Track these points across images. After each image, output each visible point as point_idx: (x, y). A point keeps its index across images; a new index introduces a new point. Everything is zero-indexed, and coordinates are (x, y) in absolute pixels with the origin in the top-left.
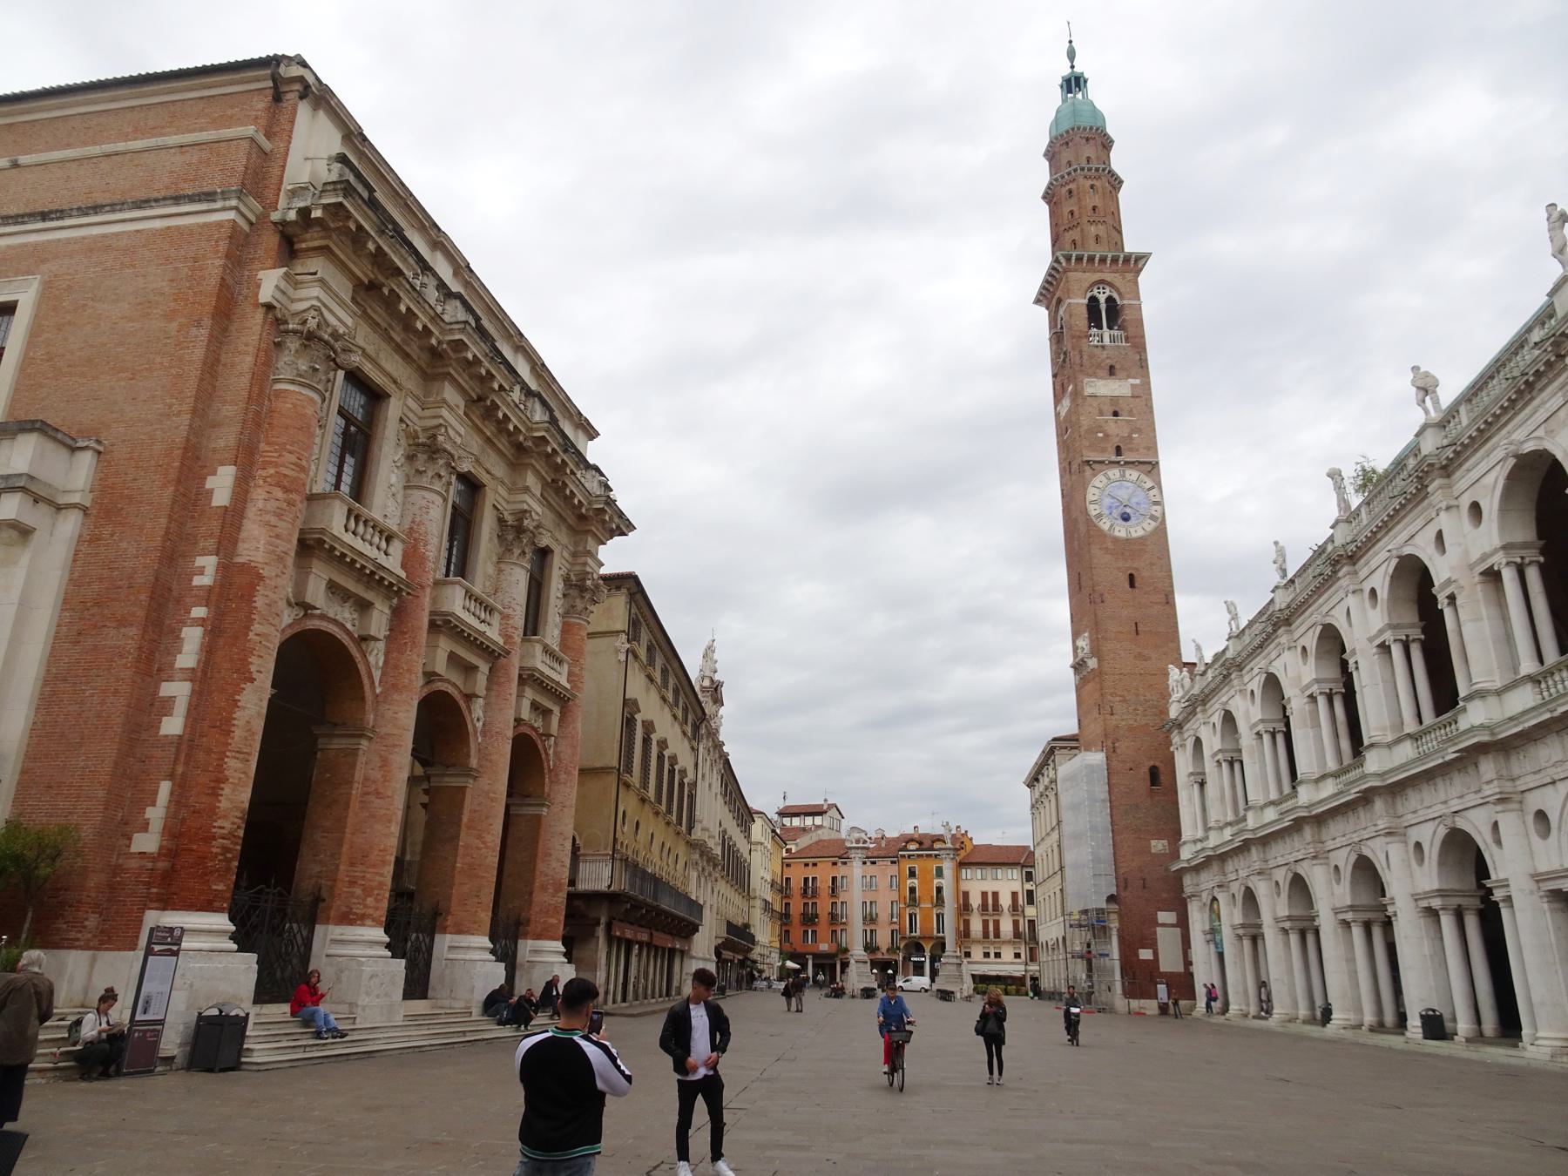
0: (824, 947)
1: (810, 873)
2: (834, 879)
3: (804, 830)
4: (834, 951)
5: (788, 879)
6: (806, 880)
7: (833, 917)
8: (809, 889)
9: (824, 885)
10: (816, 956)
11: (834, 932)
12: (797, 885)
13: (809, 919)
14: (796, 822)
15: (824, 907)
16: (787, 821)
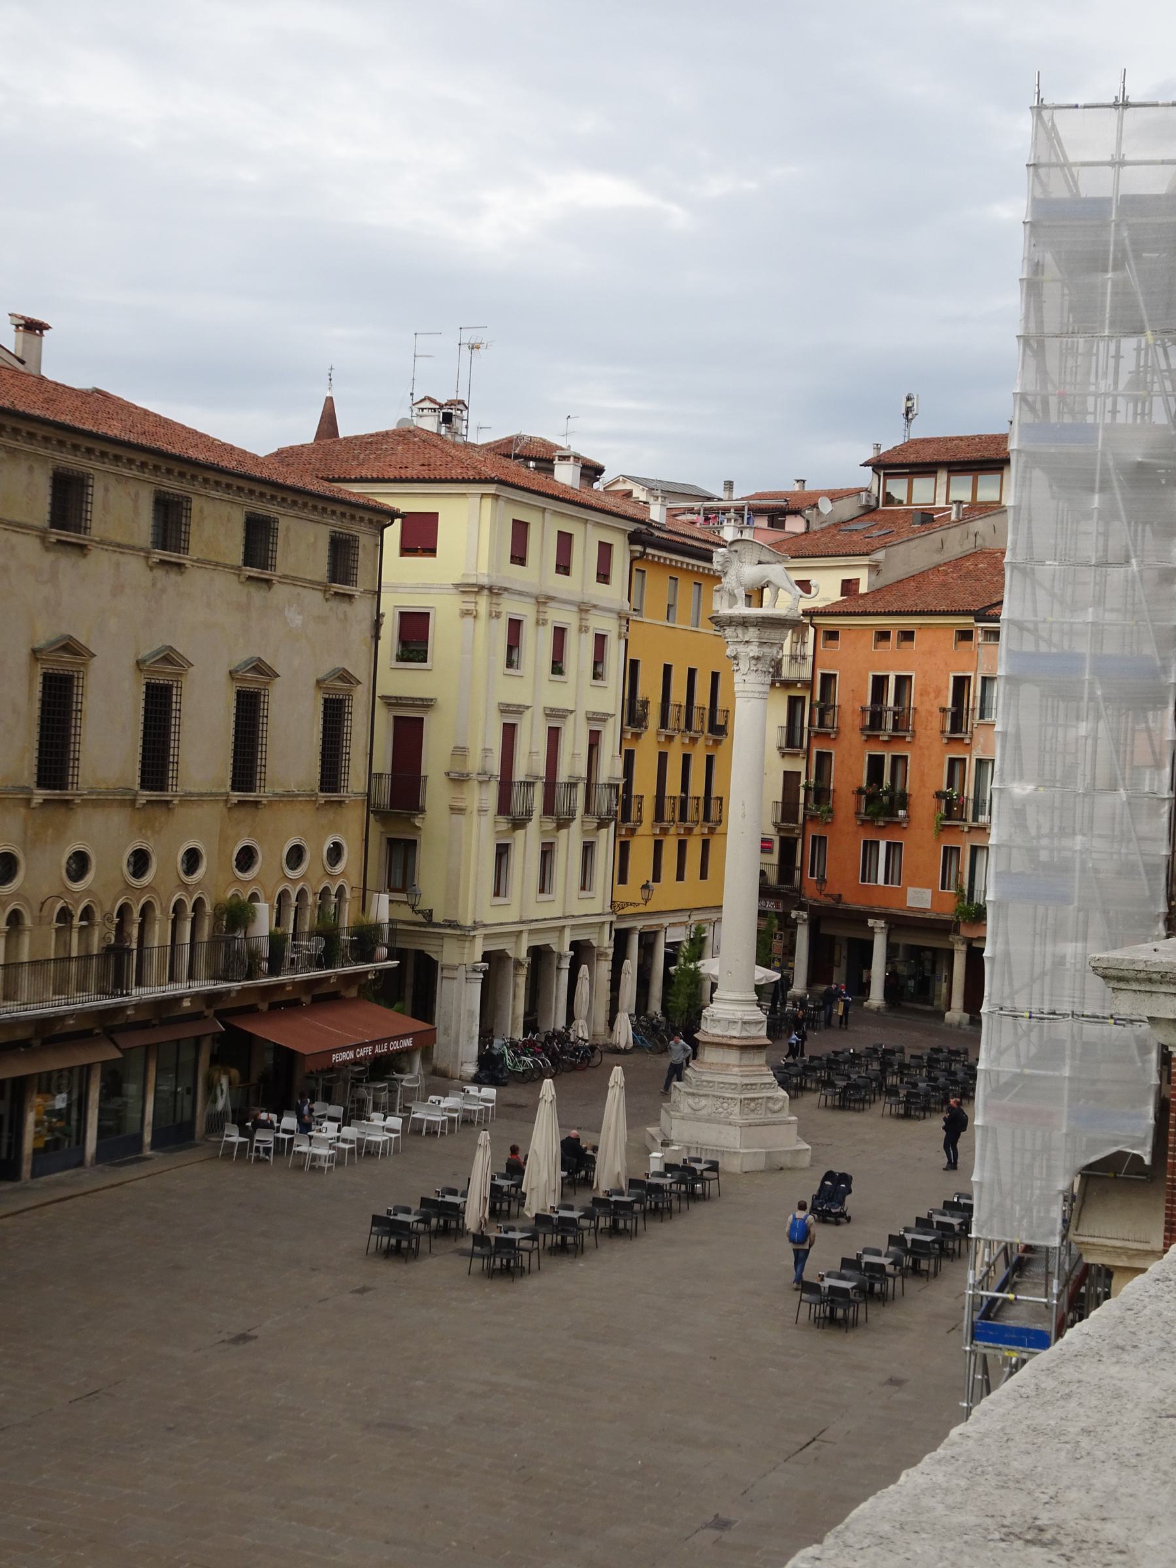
0: (919, 898)
1: (892, 662)
2: (961, 683)
3: (927, 517)
4: (947, 911)
5: (828, 679)
6: (880, 683)
7: (952, 808)
8: (888, 709)
9: (930, 702)
10: (898, 923)
11: (950, 853)
12: (852, 696)
13: (883, 802)
14: (926, 492)
15: (925, 776)
16: (898, 488)
